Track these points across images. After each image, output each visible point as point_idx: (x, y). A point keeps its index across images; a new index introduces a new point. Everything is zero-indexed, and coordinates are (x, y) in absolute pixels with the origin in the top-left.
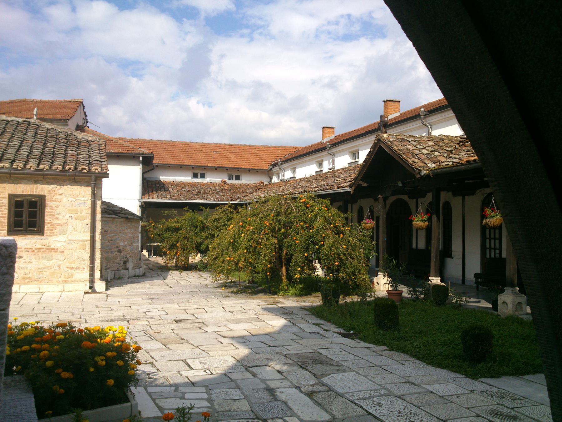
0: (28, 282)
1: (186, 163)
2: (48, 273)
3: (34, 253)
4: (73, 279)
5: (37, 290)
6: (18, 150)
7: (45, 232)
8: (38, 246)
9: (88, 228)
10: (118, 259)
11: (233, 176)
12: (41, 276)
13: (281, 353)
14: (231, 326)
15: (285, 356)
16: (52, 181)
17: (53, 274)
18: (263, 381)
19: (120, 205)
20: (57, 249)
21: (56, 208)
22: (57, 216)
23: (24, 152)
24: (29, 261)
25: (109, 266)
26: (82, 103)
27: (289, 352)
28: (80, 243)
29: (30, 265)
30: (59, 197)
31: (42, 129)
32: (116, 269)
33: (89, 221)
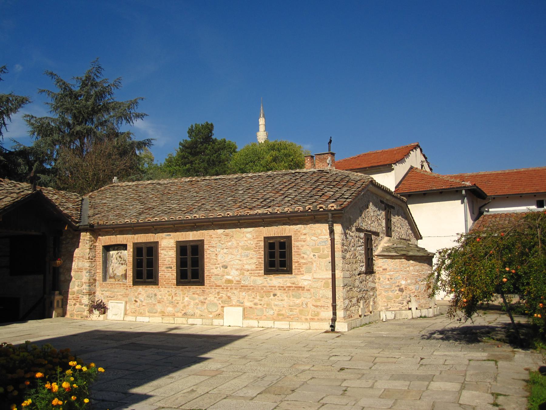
0: (282, 319)
1: (528, 190)
2: (297, 310)
3: (285, 291)
4: (318, 317)
5: (287, 327)
7: (293, 271)
8: (289, 285)
10: (400, 299)
12: (291, 313)
16: (298, 222)
17: (301, 312)
20: (304, 288)
21: (301, 248)
22: (303, 255)
24: (282, 298)
25: (389, 306)
28: (324, 281)
29: (283, 302)
30: (303, 237)
32: (398, 309)
33: (330, 259)
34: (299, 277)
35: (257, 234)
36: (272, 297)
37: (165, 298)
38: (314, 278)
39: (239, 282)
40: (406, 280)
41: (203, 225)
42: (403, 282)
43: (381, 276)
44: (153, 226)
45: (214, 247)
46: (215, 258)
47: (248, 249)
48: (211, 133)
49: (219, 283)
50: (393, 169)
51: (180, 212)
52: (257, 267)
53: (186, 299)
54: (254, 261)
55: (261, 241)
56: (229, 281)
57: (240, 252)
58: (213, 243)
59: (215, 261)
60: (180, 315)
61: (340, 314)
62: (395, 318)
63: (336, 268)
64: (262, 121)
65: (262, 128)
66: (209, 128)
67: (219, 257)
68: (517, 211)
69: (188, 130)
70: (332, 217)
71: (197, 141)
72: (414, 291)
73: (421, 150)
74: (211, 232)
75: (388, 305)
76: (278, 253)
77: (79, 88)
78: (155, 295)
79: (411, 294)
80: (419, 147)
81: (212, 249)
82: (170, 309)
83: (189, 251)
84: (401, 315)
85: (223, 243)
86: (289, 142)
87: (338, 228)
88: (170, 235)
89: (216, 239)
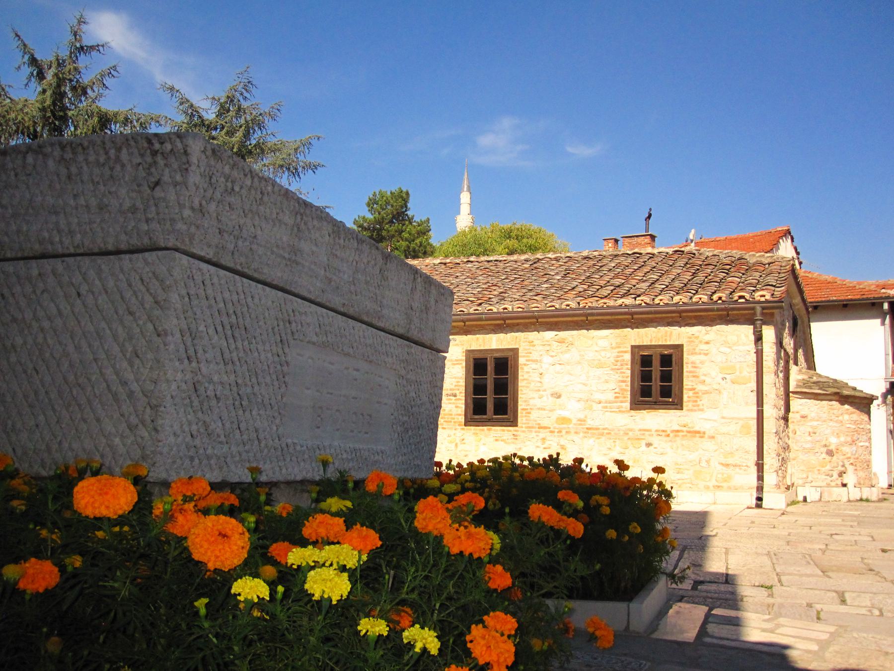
3: (668, 439)
9: (753, 397)
10: (828, 467)
12: (679, 476)
16: (694, 321)
19: (833, 376)
20: (704, 433)
22: (702, 378)
25: (810, 479)
28: (741, 422)
32: (824, 484)
33: (753, 385)
34: (697, 415)
35: (619, 340)
36: (644, 448)
38: (723, 418)
39: (582, 421)
40: (838, 436)
41: (518, 324)
43: (796, 428)
45: (536, 361)
46: (539, 379)
47: (600, 366)
48: (406, 207)
49: (545, 423)
51: (467, 302)
52: (616, 397)
54: (612, 386)
55: (626, 352)
56: (564, 420)
58: (535, 356)
59: (539, 384)
61: (770, 478)
62: (820, 500)
63: (765, 401)
64: (465, 197)
65: (465, 208)
66: (403, 198)
69: (367, 200)
70: (762, 314)
71: (383, 218)
72: (849, 455)
73: (792, 240)
74: (533, 336)
75: (808, 477)
77: (214, 116)
79: (845, 461)
80: (790, 233)
81: (534, 366)
83: (490, 368)
85: (553, 354)
86: (535, 227)
87: (769, 333)
89: (541, 348)
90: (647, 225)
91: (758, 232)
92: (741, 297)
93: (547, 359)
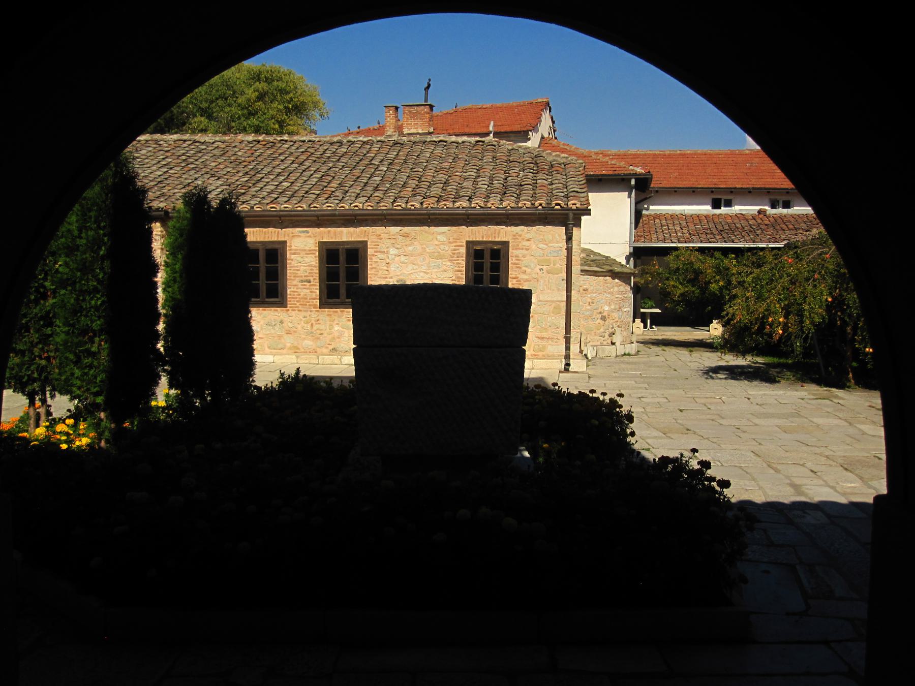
1: (702, 184)
6: (475, 182)
9: (564, 285)
10: (602, 330)
11: (778, 201)
13: (821, 454)
14: (757, 421)
15: (827, 457)
16: (518, 222)
18: (787, 477)
22: (524, 268)
23: (483, 186)
26: (548, 104)
27: (831, 453)
28: (553, 305)
31: (501, 150)
32: (599, 343)
33: (564, 275)
35: (455, 236)
37: (299, 327)
40: (610, 305)
41: (366, 220)
42: (606, 308)
44: (280, 216)
47: (440, 257)
50: (529, 139)
53: (336, 328)
57: (427, 261)
58: (382, 247)
60: (325, 351)
61: (575, 348)
67: (393, 268)
68: (686, 212)
74: (380, 230)
76: (489, 265)
78: (282, 322)
81: (380, 256)
82: (308, 343)
83: (342, 258)
84: (603, 351)
86: (285, 69)
88: (308, 232)
89: (388, 241)
90: (426, 95)
91: (521, 101)
92: (557, 204)
93: (393, 251)
